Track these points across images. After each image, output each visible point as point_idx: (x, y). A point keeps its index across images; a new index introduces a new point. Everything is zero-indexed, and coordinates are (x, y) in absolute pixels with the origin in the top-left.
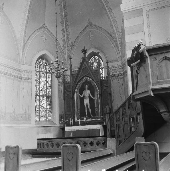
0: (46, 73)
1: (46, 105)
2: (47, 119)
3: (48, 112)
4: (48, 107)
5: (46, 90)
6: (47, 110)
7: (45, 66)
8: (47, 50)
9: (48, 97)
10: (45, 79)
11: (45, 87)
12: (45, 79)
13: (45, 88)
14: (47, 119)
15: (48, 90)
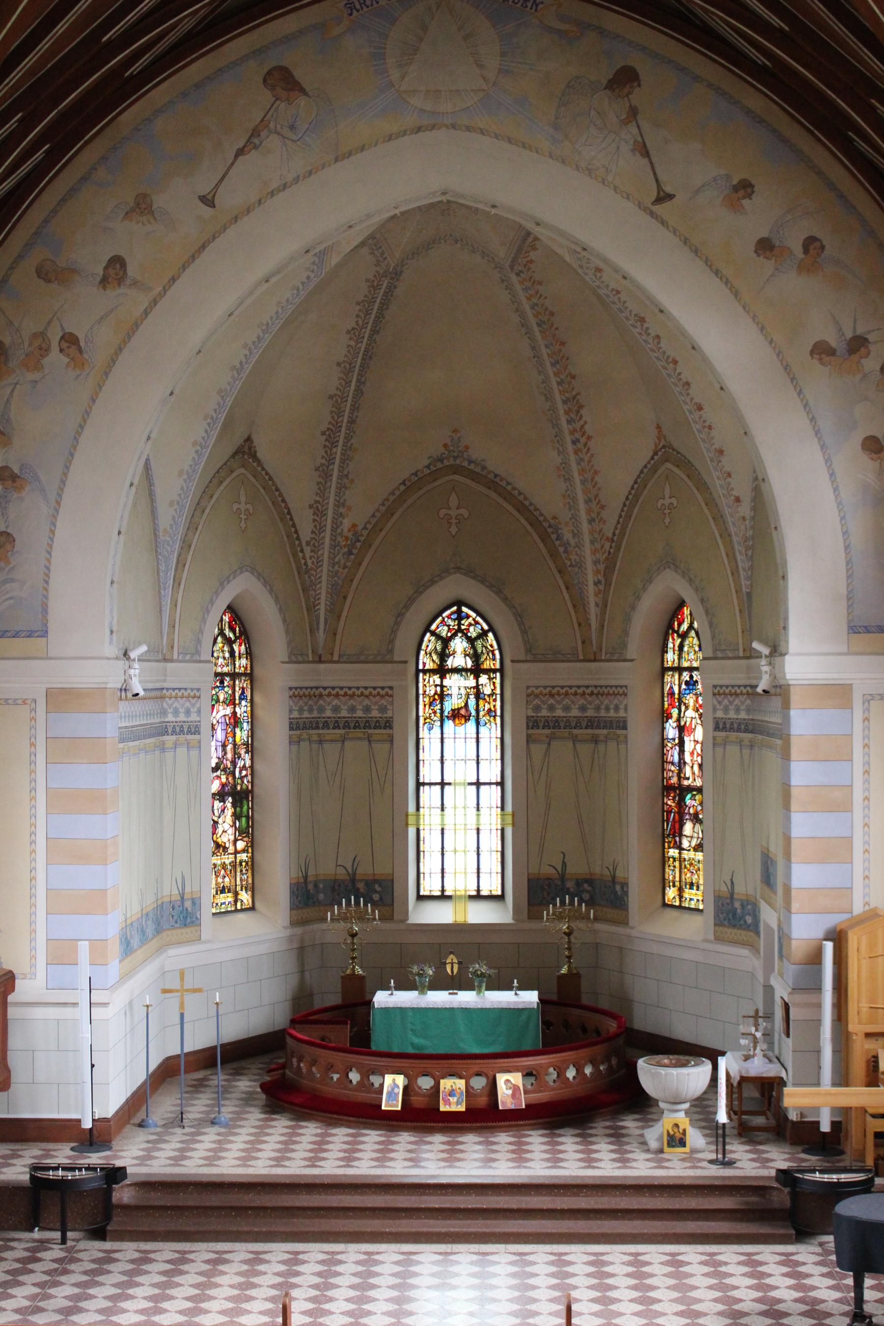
0: (234, 676)
1: (232, 838)
2: (236, 901)
3: (238, 870)
4: (241, 845)
5: (234, 763)
6: (236, 858)
7: (229, 642)
8: (253, 570)
9: (239, 796)
10: (229, 711)
11: (229, 748)
12: (229, 711)
13: (229, 756)
14: (236, 901)
15: (240, 763)
